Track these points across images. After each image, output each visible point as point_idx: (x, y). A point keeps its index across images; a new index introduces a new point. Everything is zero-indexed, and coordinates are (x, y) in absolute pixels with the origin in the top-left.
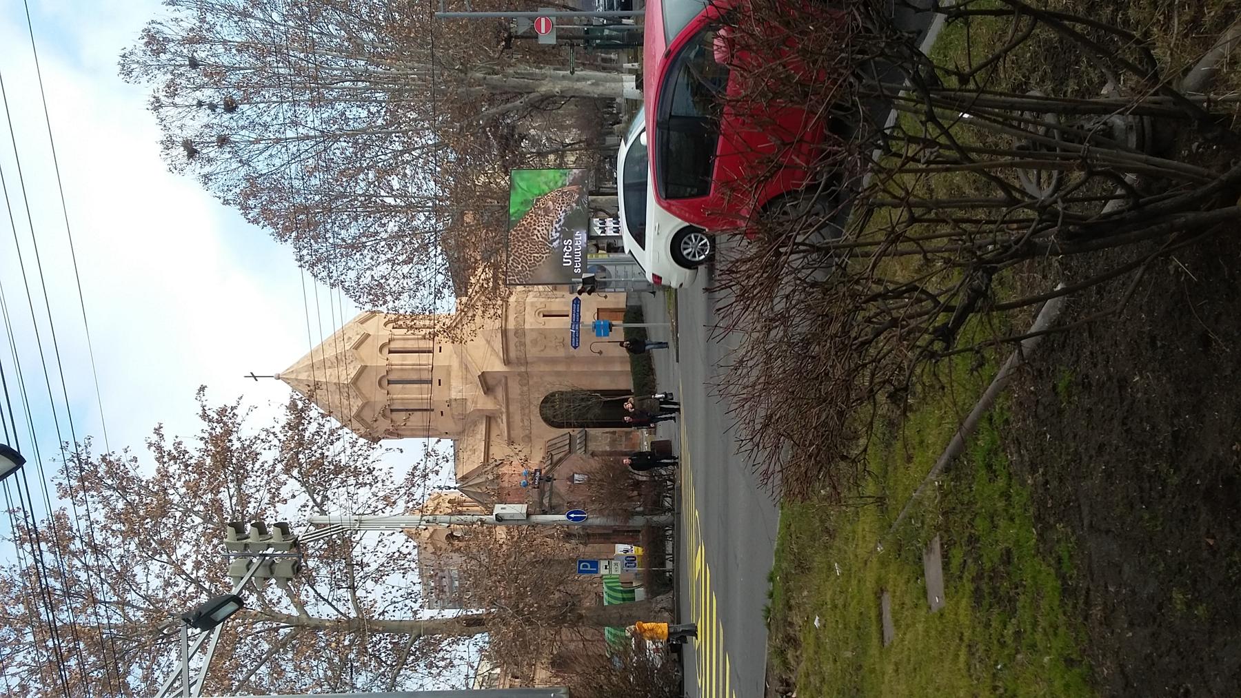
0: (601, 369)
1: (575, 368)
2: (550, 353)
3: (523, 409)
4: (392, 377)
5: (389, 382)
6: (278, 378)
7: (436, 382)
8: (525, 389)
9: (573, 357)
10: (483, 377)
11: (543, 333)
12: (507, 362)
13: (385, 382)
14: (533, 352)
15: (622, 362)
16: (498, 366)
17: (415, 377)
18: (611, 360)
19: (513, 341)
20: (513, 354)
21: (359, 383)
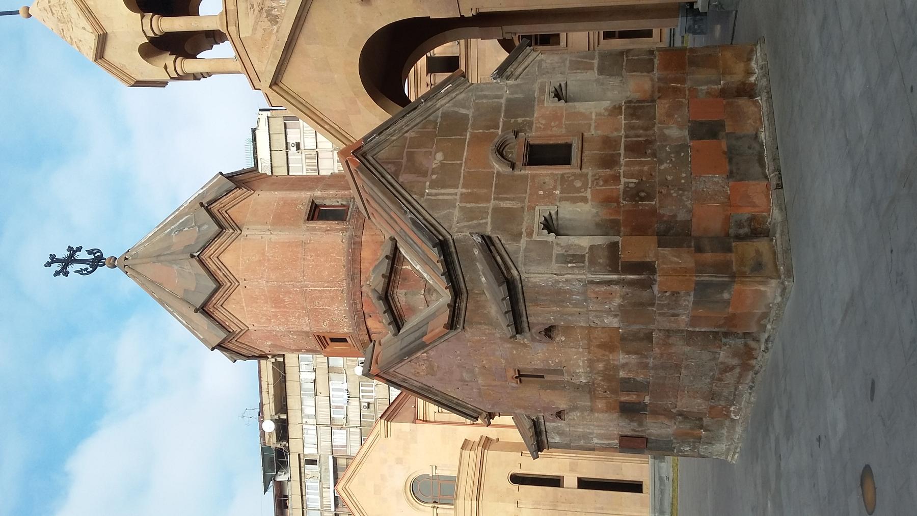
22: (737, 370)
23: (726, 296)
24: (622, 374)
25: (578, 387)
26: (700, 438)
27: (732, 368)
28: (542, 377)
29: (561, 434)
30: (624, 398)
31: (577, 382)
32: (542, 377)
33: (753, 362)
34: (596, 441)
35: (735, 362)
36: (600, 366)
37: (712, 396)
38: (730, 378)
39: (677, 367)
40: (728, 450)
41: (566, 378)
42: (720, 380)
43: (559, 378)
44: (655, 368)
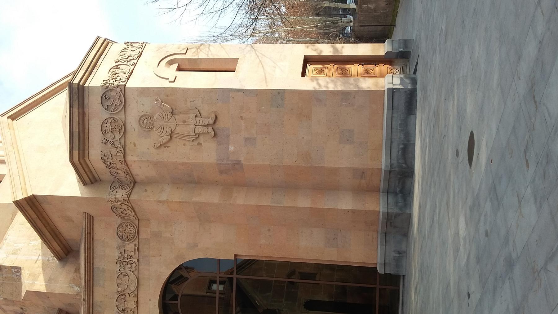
0: (304, 202)
1: (241, 199)
2: (181, 153)
3: (122, 295)
8: (130, 247)
9: (237, 165)
11: (169, 101)
12: (87, 175)
14: (142, 151)
15: (360, 191)
18: (325, 182)
19: (97, 116)
20: (95, 153)
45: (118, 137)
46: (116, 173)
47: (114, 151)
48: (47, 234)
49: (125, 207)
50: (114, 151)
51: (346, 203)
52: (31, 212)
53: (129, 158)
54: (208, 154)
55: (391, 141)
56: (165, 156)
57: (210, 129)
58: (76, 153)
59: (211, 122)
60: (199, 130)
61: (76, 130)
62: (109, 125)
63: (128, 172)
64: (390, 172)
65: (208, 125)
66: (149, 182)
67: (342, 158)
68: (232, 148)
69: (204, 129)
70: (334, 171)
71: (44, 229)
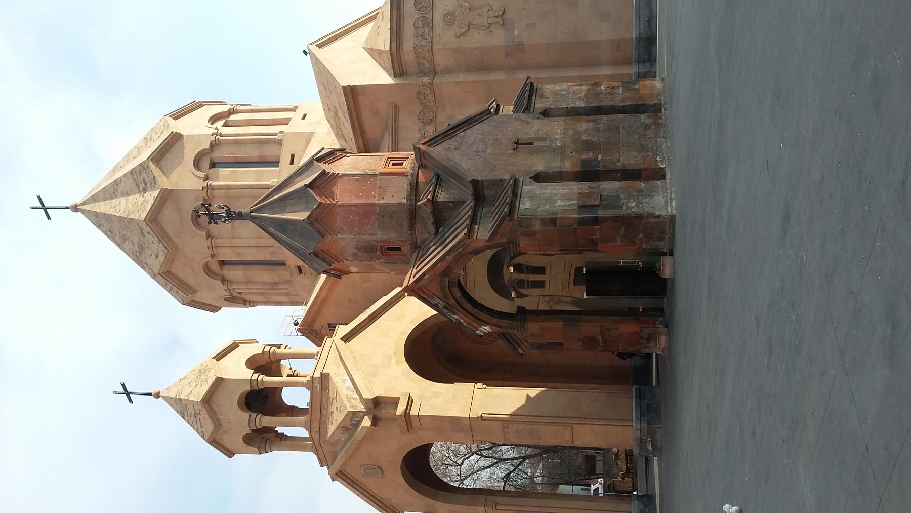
2: (477, 39)
4: (218, 155)
5: (213, 165)
6: (75, 208)
7: (285, 160)
9: (520, 47)
10: (352, 93)
12: (398, 69)
13: (206, 163)
15: (616, 63)
16: (383, 77)
17: (252, 153)
20: (408, 44)
21: (163, 162)
22: (653, 127)
23: (637, 86)
24: (584, 137)
25: (554, 150)
26: (641, 191)
27: (650, 127)
28: (532, 144)
29: (531, 198)
30: (583, 157)
31: (553, 145)
32: (532, 144)
33: (660, 121)
34: (559, 203)
35: (650, 121)
36: (571, 132)
37: (642, 148)
38: (650, 133)
39: (618, 128)
40: (666, 202)
41: (547, 143)
42: (645, 135)
43: (543, 144)
44: (604, 131)
45: (427, 31)
46: (422, 64)
47: (424, 42)
48: (357, 128)
49: (428, 91)
50: (424, 42)
51: (606, 71)
52: (351, 100)
53: (435, 47)
54: (498, 38)
55: (639, 16)
56: (464, 43)
57: (500, 19)
58: (394, 44)
59: (500, 13)
60: (491, 20)
61: (395, 27)
62: (420, 22)
63: (432, 62)
64: (639, 39)
65: (498, 17)
66: (448, 71)
67: (603, 32)
68: (516, 33)
69: (495, 20)
70: (596, 44)
71: (356, 123)
